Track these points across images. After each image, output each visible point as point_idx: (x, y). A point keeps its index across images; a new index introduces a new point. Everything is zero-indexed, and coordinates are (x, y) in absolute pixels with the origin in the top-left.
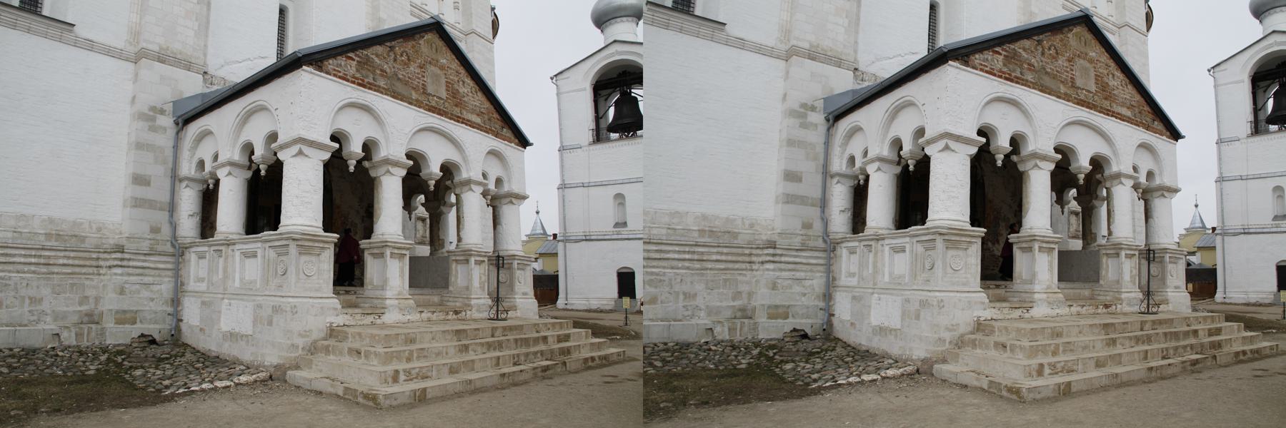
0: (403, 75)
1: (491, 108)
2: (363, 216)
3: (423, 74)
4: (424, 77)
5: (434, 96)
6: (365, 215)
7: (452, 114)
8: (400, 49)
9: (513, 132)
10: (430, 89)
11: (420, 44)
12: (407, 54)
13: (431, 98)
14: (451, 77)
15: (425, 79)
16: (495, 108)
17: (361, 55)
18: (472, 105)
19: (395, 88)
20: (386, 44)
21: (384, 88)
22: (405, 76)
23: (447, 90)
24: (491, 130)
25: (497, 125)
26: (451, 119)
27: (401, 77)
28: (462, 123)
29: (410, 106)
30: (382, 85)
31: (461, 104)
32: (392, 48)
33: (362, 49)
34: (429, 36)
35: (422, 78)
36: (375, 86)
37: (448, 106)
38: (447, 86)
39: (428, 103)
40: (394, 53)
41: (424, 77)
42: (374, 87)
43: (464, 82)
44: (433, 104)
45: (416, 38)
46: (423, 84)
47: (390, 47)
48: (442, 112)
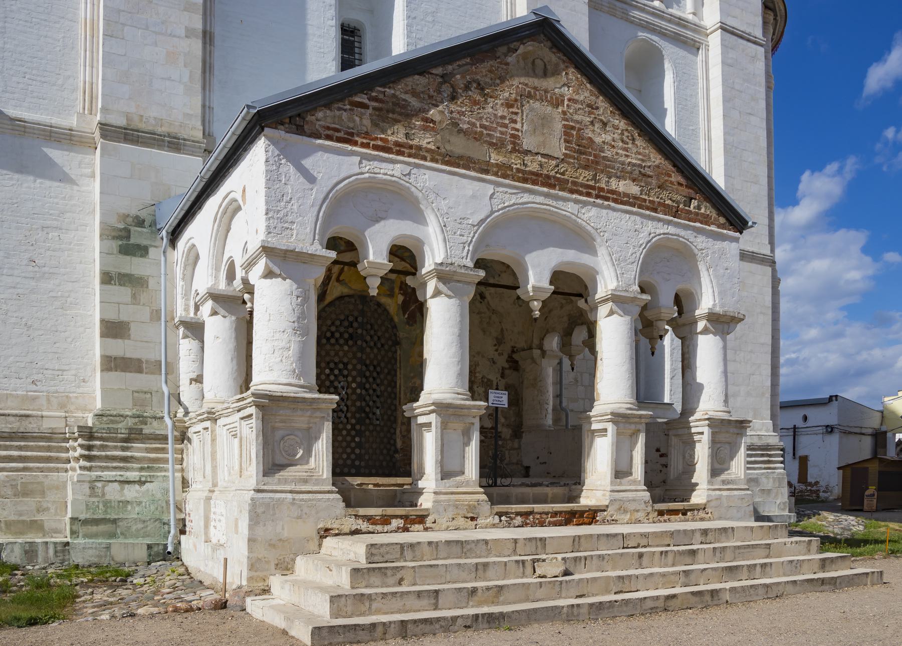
0: (468, 123)
2: (503, 369)
3: (514, 117)
4: (515, 122)
5: (537, 154)
6: (506, 365)
7: (574, 183)
8: (463, 77)
10: (527, 143)
11: (507, 64)
12: (479, 84)
13: (528, 159)
14: (576, 117)
15: (518, 126)
16: (675, 166)
17: (381, 96)
18: (623, 163)
20: (434, 71)
21: (428, 150)
22: (474, 125)
23: (566, 141)
24: (664, 205)
26: (572, 192)
27: (465, 126)
28: (597, 197)
29: (484, 176)
30: (425, 145)
31: (597, 163)
32: (445, 78)
33: (384, 86)
34: (529, 47)
35: (513, 125)
36: (411, 147)
37: (570, 173)
38: (566, 133)
39: (523, 168)
40: (452, 86)
41: (515, 122)
42: (406, 151)
43: (605, 124)
44: (533, 167)
45: (498, 54)
46: (513, 136)
47: (442, 77)
48: (552, 181)
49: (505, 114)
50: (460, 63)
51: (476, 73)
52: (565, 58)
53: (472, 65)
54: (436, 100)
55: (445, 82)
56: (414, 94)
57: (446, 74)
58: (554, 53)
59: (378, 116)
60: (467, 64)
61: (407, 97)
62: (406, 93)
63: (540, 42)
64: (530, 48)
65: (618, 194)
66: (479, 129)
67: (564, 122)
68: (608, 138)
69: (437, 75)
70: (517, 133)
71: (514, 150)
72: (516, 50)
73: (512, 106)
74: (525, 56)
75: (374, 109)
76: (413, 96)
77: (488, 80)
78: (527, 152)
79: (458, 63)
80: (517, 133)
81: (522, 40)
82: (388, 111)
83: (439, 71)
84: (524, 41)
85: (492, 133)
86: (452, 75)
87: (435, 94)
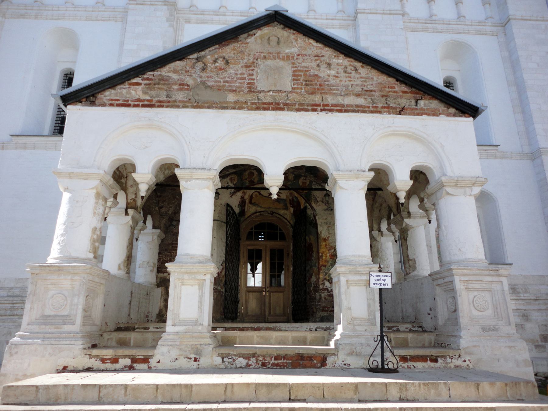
1: (392, 81)
3: (251, 72)
9: (441, 101)
10: (260, 86)
13: (261, 96)
15: (254, 77)
17: (151, 77)
19: (196, 97)
25: (406, 101)
40: (204, 63)
43: (329, 65)
46: (249, 83)
47: (197, 59)
48: (282, 106)
49: (244, 72)
50: (211, 49)
51: (222, 52)
52: (294, 32)
53: (219, 48)
54: (191, 73)
55: (198, 61)
56: (175, 71)
57: (200, 57)
58: (286, 31)
59: (147, 88)
60: (215, 49)
61: (170, 74)
62: (169, 72)
63: (275, 26)
64: (266, 31)
65: (343, 106)
66: (222, 84)
67: (293, 69)
68: (333, 72)
69: (193, 59)
70: (253, 81)
71: (250, 92)
72: (255, 35)
73: (250, 66)
74: (262, 37)
75: (146, 84)
76: (174, 73)
77: (232, 55)
78: (260, 92)
79: (209, 49)
80: (253, 81)
81: (259, 27)
82: (155, 84)
83: (195, 56)
84: (261, 28)
85: (231, 84)
86: (204, 56)
87: (191, 69)
